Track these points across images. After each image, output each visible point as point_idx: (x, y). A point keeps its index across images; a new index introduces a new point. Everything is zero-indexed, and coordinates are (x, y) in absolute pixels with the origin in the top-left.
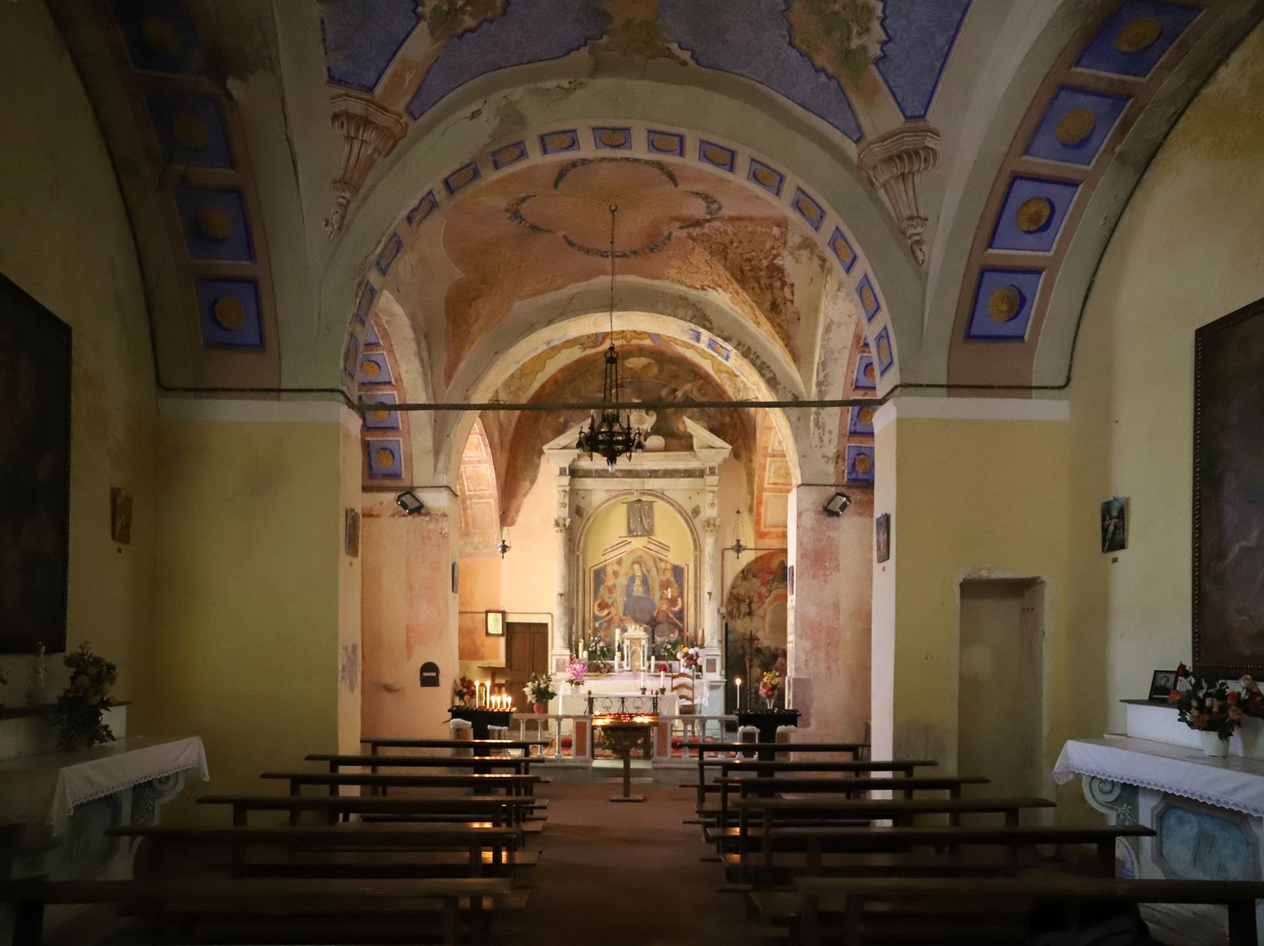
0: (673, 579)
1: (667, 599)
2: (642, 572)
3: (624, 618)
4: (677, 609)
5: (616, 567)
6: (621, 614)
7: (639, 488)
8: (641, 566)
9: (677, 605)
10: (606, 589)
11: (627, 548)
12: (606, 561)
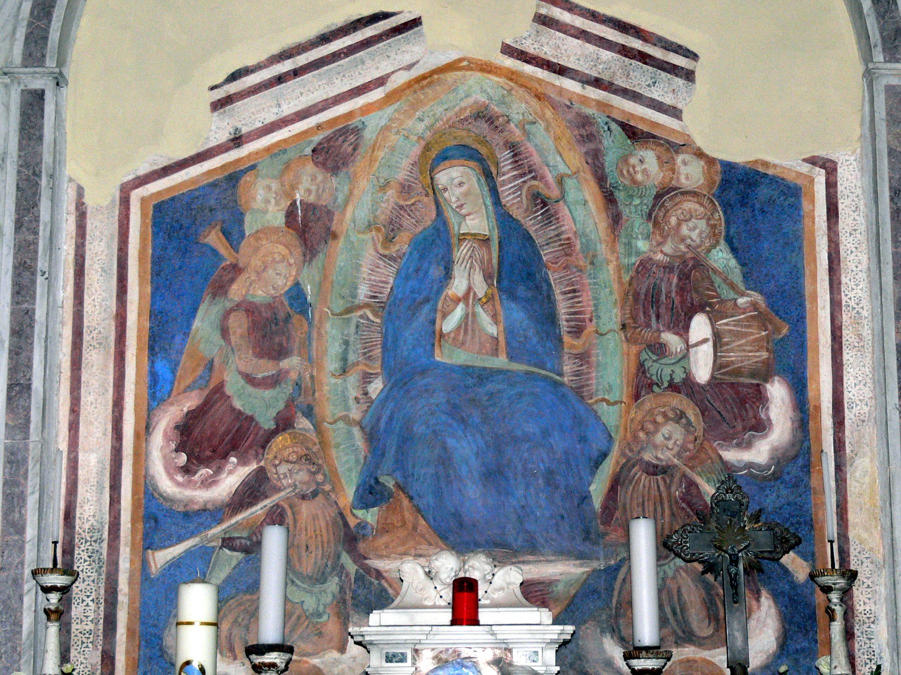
2: (505, 219)
3: (371, 516)
6: (349, 493)
8: (488, 176)
9: (761, 427)
10: (239, 324)
12: (237, 141)
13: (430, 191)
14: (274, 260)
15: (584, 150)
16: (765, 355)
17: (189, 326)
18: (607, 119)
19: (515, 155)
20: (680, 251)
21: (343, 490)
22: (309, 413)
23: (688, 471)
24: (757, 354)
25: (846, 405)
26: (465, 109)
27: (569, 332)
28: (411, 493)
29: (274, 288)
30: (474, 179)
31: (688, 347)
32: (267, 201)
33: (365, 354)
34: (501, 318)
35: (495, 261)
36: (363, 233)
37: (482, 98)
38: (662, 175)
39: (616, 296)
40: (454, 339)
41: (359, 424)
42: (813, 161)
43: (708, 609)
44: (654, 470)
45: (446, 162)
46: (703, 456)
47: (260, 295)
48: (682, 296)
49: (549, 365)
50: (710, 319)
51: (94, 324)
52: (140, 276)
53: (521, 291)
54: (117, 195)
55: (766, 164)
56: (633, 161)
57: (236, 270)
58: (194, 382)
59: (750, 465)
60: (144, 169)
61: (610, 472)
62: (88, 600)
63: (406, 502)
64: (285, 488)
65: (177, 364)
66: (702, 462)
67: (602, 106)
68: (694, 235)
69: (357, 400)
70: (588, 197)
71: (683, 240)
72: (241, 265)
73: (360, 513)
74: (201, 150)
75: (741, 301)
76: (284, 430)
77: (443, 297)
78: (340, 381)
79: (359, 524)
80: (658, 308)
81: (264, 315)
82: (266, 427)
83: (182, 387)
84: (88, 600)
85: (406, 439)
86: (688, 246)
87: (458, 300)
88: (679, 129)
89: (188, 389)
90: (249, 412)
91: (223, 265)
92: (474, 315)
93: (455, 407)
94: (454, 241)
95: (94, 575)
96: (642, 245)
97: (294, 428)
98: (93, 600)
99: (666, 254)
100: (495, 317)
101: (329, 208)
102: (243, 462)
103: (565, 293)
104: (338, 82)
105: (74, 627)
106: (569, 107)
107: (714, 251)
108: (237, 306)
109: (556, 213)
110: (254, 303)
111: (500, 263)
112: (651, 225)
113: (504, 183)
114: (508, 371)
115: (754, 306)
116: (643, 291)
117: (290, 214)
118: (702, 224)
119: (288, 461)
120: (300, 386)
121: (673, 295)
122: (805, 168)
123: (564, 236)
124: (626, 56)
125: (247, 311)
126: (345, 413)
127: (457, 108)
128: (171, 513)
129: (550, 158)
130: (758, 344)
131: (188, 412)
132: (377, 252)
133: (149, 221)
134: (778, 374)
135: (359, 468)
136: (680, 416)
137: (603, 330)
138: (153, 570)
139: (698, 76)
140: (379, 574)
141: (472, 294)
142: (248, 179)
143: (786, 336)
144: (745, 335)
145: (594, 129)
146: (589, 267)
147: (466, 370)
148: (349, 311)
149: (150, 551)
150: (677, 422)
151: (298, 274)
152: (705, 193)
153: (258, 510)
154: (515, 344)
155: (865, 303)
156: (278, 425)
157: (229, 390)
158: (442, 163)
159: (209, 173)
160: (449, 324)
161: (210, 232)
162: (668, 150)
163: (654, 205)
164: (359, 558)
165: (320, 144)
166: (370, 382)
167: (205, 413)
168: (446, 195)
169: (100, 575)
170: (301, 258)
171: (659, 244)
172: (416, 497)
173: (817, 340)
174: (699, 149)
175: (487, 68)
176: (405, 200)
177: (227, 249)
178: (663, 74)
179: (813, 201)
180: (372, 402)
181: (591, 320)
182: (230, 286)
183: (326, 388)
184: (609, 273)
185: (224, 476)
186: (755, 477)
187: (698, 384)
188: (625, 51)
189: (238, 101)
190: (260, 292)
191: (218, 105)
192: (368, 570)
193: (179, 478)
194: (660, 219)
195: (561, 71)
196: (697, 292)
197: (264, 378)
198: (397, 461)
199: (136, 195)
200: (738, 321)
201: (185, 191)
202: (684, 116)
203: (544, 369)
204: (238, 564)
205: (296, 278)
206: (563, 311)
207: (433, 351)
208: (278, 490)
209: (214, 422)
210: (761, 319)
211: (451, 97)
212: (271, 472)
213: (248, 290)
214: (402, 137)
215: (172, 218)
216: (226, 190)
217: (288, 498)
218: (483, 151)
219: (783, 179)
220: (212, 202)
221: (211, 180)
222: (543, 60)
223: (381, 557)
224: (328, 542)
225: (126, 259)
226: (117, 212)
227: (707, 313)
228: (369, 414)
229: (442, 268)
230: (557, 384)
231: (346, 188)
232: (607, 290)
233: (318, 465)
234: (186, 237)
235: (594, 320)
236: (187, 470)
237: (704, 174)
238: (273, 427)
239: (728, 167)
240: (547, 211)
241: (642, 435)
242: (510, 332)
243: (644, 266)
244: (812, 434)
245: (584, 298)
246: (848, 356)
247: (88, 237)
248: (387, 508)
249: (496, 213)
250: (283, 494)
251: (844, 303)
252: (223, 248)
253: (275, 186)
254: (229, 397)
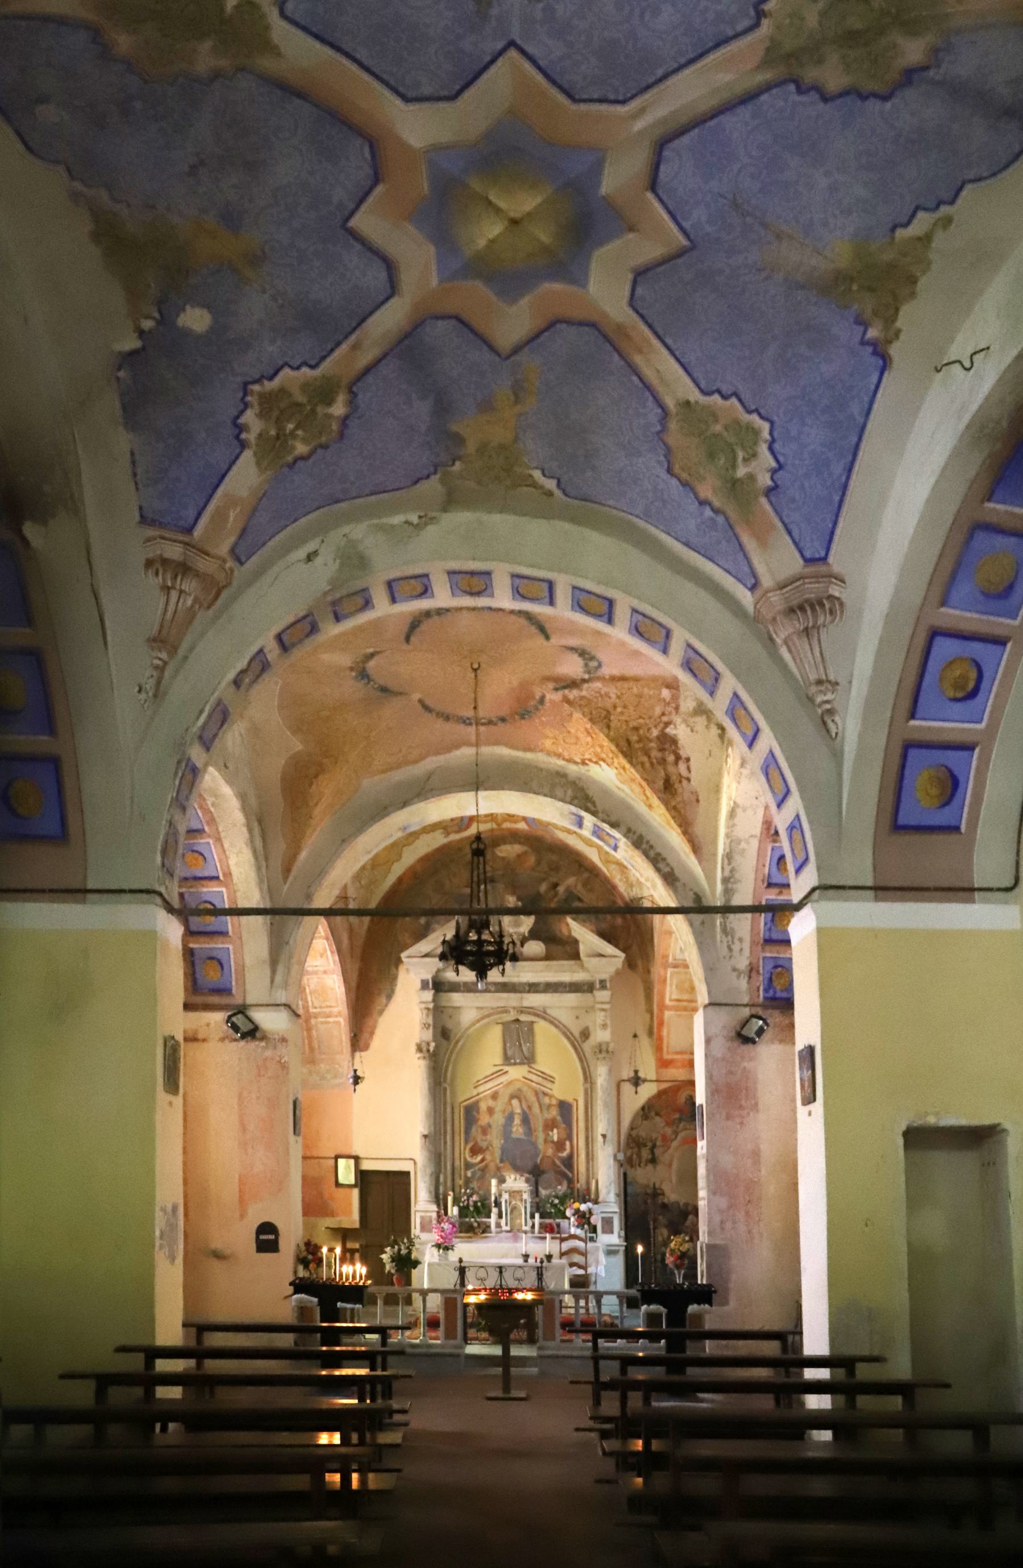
0: (559, 1118)
1: (553, 1142)
2: (522, 1109)
3: (502, 1165)
4: (565, 1154)
5: (491, 1103)
6: (498, 1161)
8: (520, 1101)
9: (565, 1149)
10: (480, 1130)
11: (504, 1079)
12: (478, 1094)
42: (575, 1100)
44: (548, 1157)
96: (546, 1115)
153: (483, 1164)
191: (476, 1087)
195: (532, 1081)
236: (472, 1156)
246: (579, 1136)
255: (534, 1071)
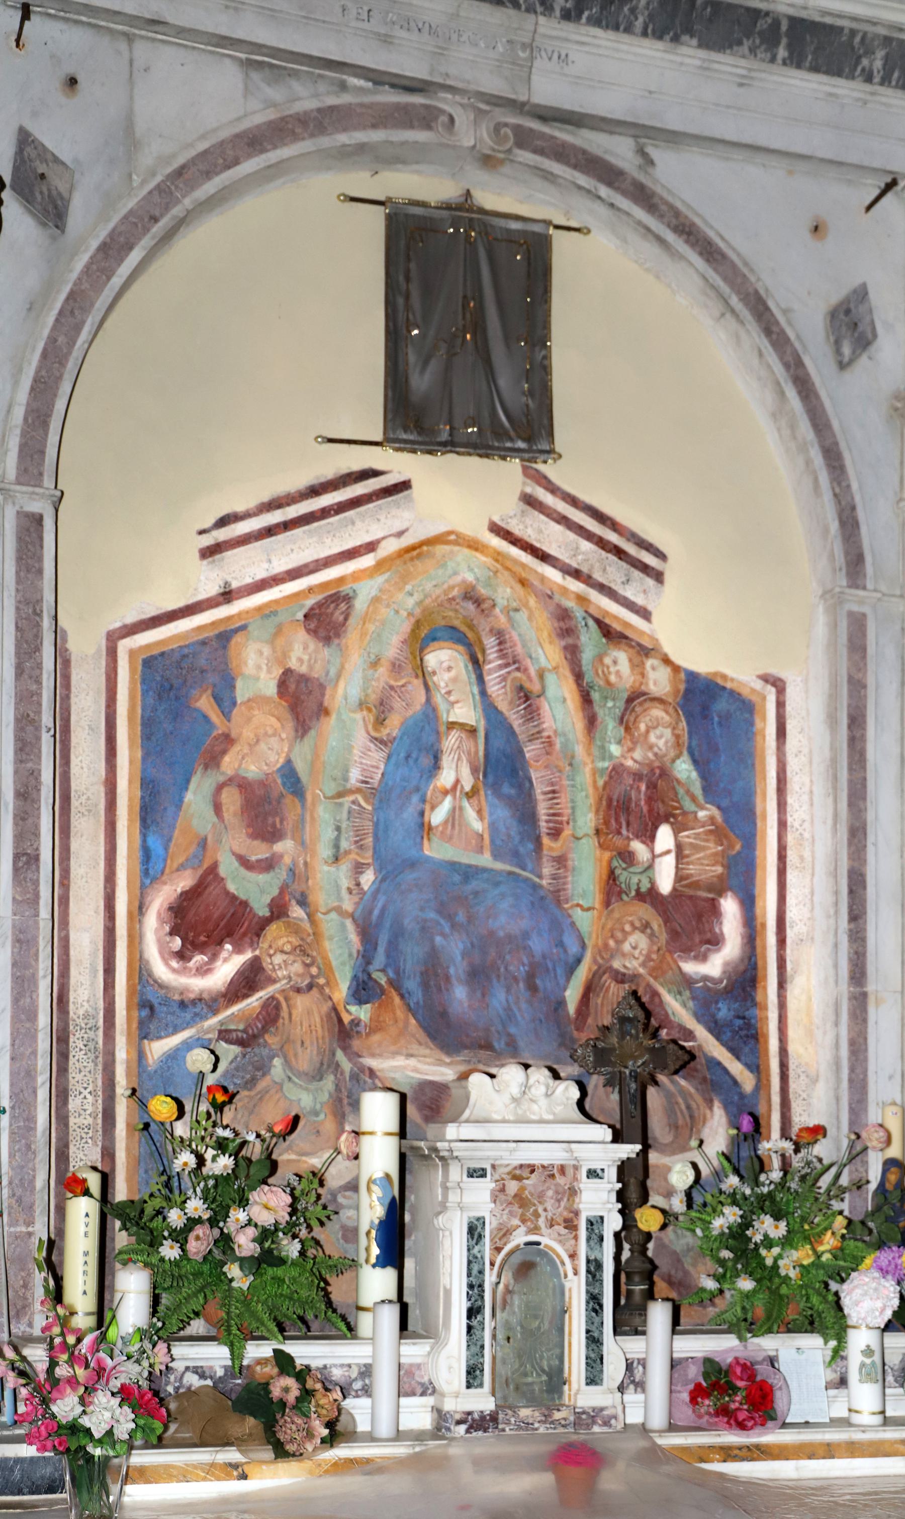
0: (684, 769)
1: (650, 896)
3: (363, 1013)
6: (342, 989)
7: (494, 85)
8: (476, 663)
9: (716, 941)
10: (231, 800)
12: (227, 596)
13: (420, 674)
14: (266, 734)
15: (563, 643)
16: (719, 869)
17: (181, 800)
18: (584, 614)
19: (500, 644)
20: (648, 758)
21: (337, 984)
22: (303, 902)
23: (652, 980)
24: (713, 868)
25: (788, 924)
26: (452, 588)
27: (548, 834)
28: (404, 991)
29: (267, 764)
30: (462, 665)
31: (654, 857)
32: (259, 668)
33: (356, 842)
34: (486, 814)
35: (481, 753)
36: (354, 712)
37: (470, 577)
38: (632, 678)
39: (591, 801)
40: (442, 833)
41: (352, 916)
42: (766, 679)
43: (669, 1117)
44: (620, 978)
45: (436, 644)
46: (665, 966)
47: (253, 770)
48: (650, 806)
49: (530, 866)
50: (673, 830)
51: (83, 788)
52: (130, 738)
53: (507, 789)
54: (104, 642)
55: (724, 677)
56: (607, 661)
57: (228, 740)
58: (187, 860)
59: (705, 978)
60: (131, 618)
61: (584, 979)
62: (86, 1093)
63: (397, 1000)
64: (280, 980)
65: (170, 840)
66: (664, 973)
67: (582, 599)
68: (661, 743)
69: (350, 891)
70: (568, 695)
71: (651, 747)
72: (233, 735)
73: (353, 1009)
74: (191, 601)
75: (702, 814)
76: (278, 917)
77: (431, 787)
78: (333, 869)
79: (353, 1021)
80: (628, 814)
81: (258, 792)
82: (261, 914)
83: (175, 865)
84: (86, 1093)
85: (398, 933)
86: (656, 755)
87: (446, 793)
88: (648, 631)
89: (181, 867)
90: (243, 897)
91: (215, 733)
92: (461, 809)
93: (442, 904)
94: (443, 729)
95: (91, 1066)
97: (288, 916)
98: (90, 1093)
99: (635, 761)
100: (479, 812)
101: (322, 680)
102: (238, 950)
103: (545, 793)
104: (328, 541)
105: (72, 1121)
106: (550, 597)
107: (678, 762)
108: (231, 780)
109: (538, 709)
110: (244, 778)
111: (486, 756)
112: (622, 730)
113: (490, 672)
114: (492, 870)
115: (712, 819)
116: (615, 797)
117: (282, 684)
118: (668, 733)
119: (282, 952)
120: (294, 874)
121: (643, 803)
122: (758, 685)
123: (545, 734)
124: (603, 548)
125: (240, 786)
126: (336, 904)
127: (445, 586)
128: (166, 1002)
129: (533, 650)
130: (715, 859)
131: (182, 894)
132: (368, 733)
133: (138, 677)
134: (731, 889)
135: (352, 962)
136: (645, 926)
137: (580, 833)
138: (150, 1061)
139: (667, 577)
140: (372, 1072)
141: (459, 787)
142: (239, 640)
143: (739, 853)
144: (703, 848)
145: (573, 623)
146: (568, 768)
147: (453, 865)
148: (340, 795)
149: (146, 1041)
150: (643, 932)
151: (290, 751)
152: (670, 700)
153: (254, 1002)
154: (498, 842)
155: (807, 825)
156: (272, 912)
157: (222, 871)
158: (431, 644)
159: (200, 629)
160: (438, 817)
161: (201, 696)
162: (638, 653)
163: (626, 709)
164: (353, 1056)
165: (312, 609)
166: (361, 873)
167: (200, 894)
168: (435, 678)
169: (96, 1065)
170: (293, 733)
171: (630, 750)
172: (407, 995)
173: (765, 858)
174: (666, 655)
175: (475, 545)
176: (396, 680)
177: (218, 716)
178: (636, 574)
179: (764, 719)
180: (365, 893)
181: (568, 823)
182: (222, 758)
183: (319, 876)
184: (585, 776)
185: (219, 963)
186: (709, 989)
187: (661, 895)
188: (601, 543)
189: (227, 550)
190: (253, 768)
191: (209, 552)
192: (362, 1069)
193: (174, 964)
194: (631, 724)
195: (544, 557)
196: (663, 802)
197: (258, 861)
198: (388, 956)
199: (125, 646)
200: (698, 834)
201: (175, 646)
202: (654, 618)
203: (524, 870)
204: (236, 1057)
205: (288, 755)
206: (543, 811)
207: (422, 844)
208: (274, 981)
209: (208, 906)
210: (717, 833)
211: (440, 572)
212: (266, 963)
213: (240, 766)
214: (392, 613)
215: (162, 676)
216: (216, 650)
217: (283, 991)
218: (470, 635)
219: (739, 694)
220: (202, 662)
221: (201, 637)
222: (527, 543)
223: (373, 1055)
224: (323, 1038)
225: (115, 719)
226: (104, 663)
227: (672, 824)
228: (361, 907)
229: (431, 757)
230: (536, 887)
231: (338, 661)
232: (584, 794)
233: (312, 957)
234: (177, 698)
235: (571, 823)
236: (181, 955)
237: (670, 681)
238: (268, 914)
239: (692, 677)
240: (529, 706)
241: (612, 943)
242: (493, 827)
243: (617, 771)
244: (759, 950)
245: (562, 800)
247: (73, 689)
248: (380, 1005)
249: (482, 702)
250: (278, 986)
251: (789, 824)
252: (215, 716)
253: (267, 651)
254: (223, 879)
255: (548, 499)
